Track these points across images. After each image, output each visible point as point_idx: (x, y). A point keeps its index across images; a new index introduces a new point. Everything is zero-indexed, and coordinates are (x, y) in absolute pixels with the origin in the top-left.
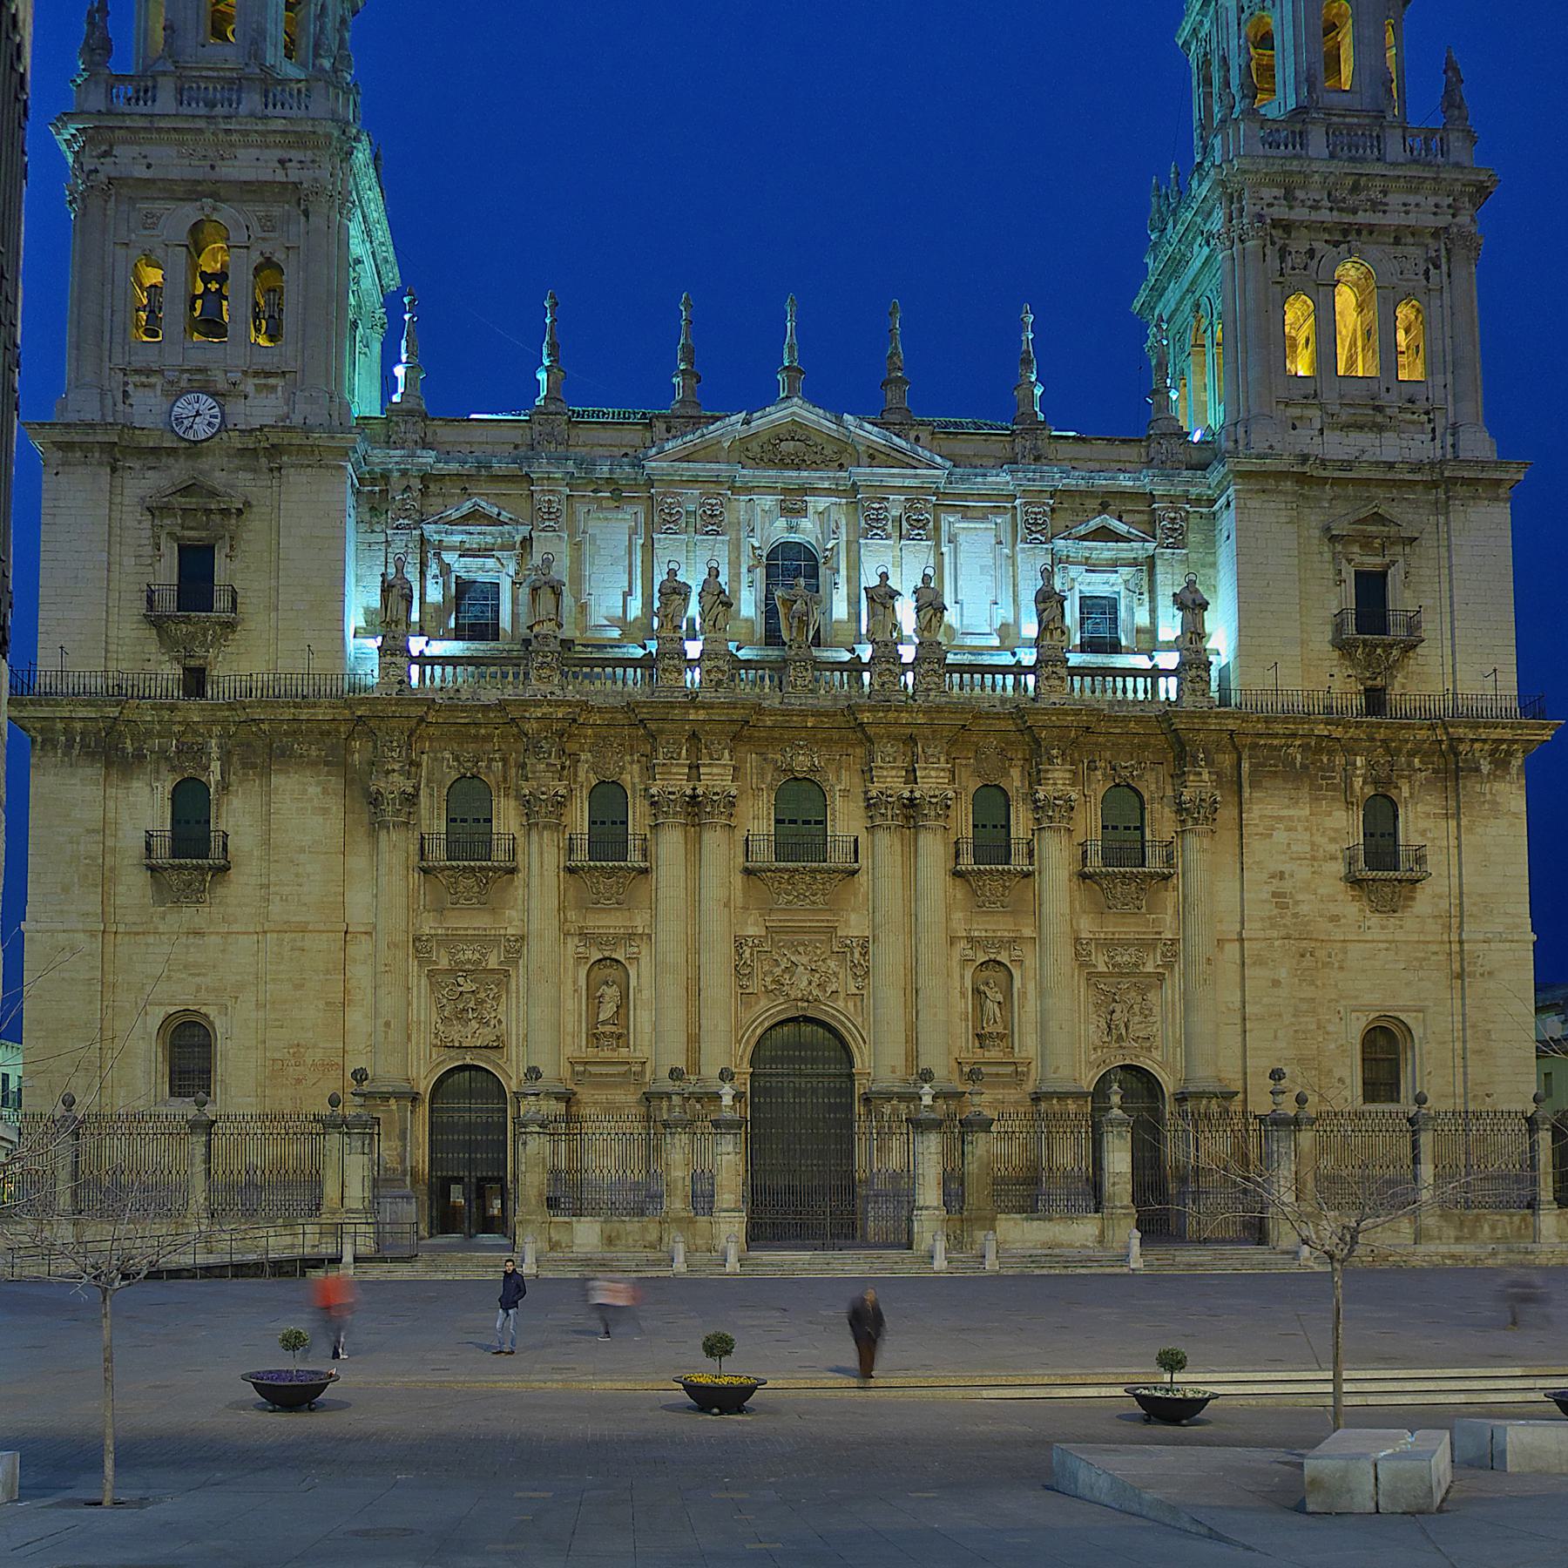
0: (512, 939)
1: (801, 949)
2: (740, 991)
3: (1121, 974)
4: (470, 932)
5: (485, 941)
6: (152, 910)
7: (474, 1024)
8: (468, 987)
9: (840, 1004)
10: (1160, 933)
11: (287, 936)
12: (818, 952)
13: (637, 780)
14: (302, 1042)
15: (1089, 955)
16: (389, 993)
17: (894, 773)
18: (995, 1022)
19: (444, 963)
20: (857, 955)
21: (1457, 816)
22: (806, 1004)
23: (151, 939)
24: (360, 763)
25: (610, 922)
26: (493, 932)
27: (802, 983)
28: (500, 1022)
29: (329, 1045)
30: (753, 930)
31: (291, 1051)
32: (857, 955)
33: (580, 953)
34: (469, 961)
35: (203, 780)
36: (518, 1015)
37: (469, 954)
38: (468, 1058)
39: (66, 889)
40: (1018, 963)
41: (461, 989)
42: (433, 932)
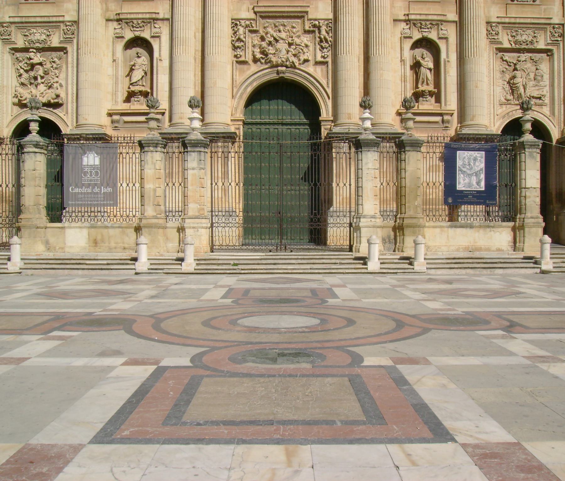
0: (68, 24)
1: (281, 28)
2: (235, 59)
4: (38, 20)
7: (42, 88)
8: (37, 58)
9: (310, 68)
10: (551, 18)
12: (294, 30)
15: (497, 34)
18: (427, 84)
19: (20, 44)
22: (284, 68)
26: (54, 19)
28: (61, 86)
34: (38, 41)
37: (37, 37)
40: (444, 41)
42: (12, 20)
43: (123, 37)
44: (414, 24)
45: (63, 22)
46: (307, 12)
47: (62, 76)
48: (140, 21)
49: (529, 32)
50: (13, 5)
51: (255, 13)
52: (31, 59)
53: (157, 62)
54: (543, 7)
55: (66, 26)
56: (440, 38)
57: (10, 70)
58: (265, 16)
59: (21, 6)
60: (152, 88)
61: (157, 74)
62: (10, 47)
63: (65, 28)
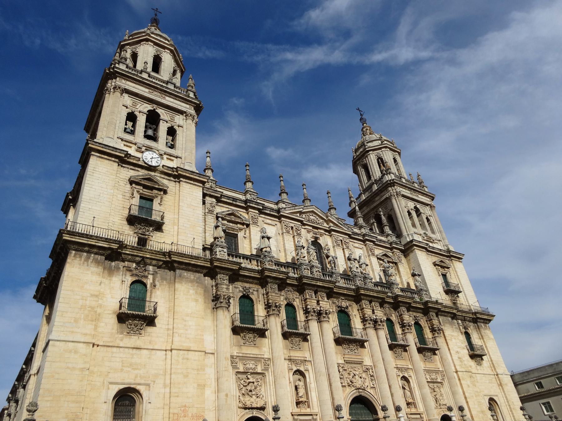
0: (267, 359)
3: (433, 382)
4: (252, 356)
5: (257, 359)
6: (117, 336)
11: (182, 352)
13: (298, 304)
14: (187, 405)
16: (227, 380)
17: (369, 310)
19: (241, 369)
20: (371, 372)
21: (483, 338)
23: (115, 350)
24: (208, 284)
25: (296, 354)
26: (259, 356)
27: (358, 383)
29: (199, 406)
30: (341, 361)
31: (182, 409)
32: (371, 372)
33: (290, 367)
34: (251, 368)
35: (145, 281)
36: (270, 393)
38: (254, 413)
39: (76, 321)
41: (249, 380)
42: (238, 355)
43: (292, 369)
44: (399, 369)
45: (263, 358)
46: (363, 362)
47: (263, 390)
48: (299, 361)
49: (434, 374)
50: (238, 346)
51: (344, 361)
52: (248, 379)
53: (309, 384)
54: (435, 363)
55: (233, 358)
56: (409, 376)
57: (234, 385)
58: (347, 362)
59: (242, 347)
60: (308, 398)
61: (310, 391)
62: (236, 371)
63: (265, 362)
